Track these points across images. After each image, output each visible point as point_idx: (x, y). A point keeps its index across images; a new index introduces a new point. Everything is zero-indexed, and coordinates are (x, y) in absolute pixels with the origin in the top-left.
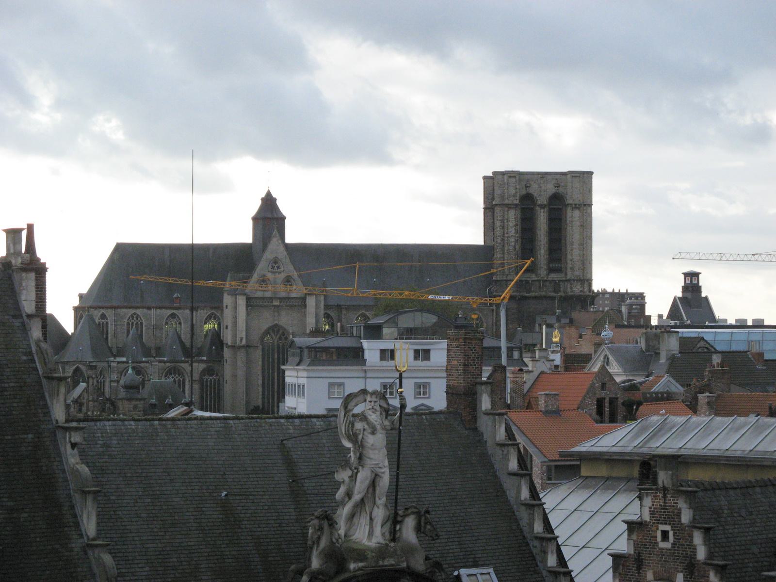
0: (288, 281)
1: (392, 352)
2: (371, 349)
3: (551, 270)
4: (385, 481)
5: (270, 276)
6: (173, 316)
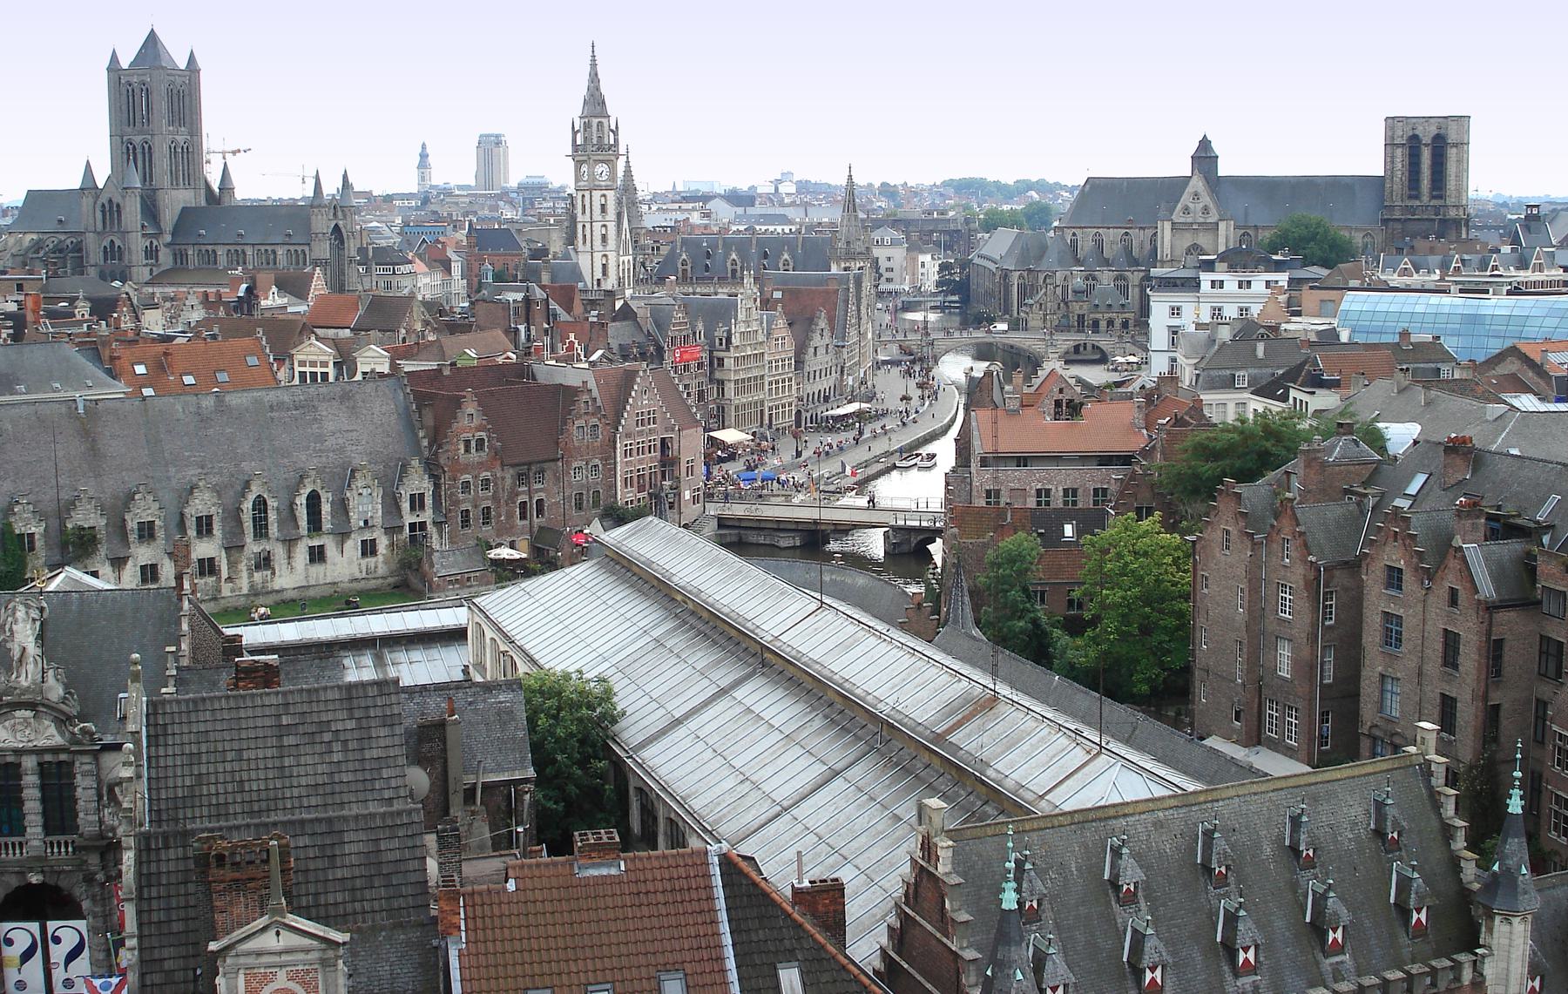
0: (1206, 210)
1: (1222, 282)
2: (1206, 278)
3: (1433, 197)
4: (32, 649)
5: (1191, 205)
6: (1127, 234)
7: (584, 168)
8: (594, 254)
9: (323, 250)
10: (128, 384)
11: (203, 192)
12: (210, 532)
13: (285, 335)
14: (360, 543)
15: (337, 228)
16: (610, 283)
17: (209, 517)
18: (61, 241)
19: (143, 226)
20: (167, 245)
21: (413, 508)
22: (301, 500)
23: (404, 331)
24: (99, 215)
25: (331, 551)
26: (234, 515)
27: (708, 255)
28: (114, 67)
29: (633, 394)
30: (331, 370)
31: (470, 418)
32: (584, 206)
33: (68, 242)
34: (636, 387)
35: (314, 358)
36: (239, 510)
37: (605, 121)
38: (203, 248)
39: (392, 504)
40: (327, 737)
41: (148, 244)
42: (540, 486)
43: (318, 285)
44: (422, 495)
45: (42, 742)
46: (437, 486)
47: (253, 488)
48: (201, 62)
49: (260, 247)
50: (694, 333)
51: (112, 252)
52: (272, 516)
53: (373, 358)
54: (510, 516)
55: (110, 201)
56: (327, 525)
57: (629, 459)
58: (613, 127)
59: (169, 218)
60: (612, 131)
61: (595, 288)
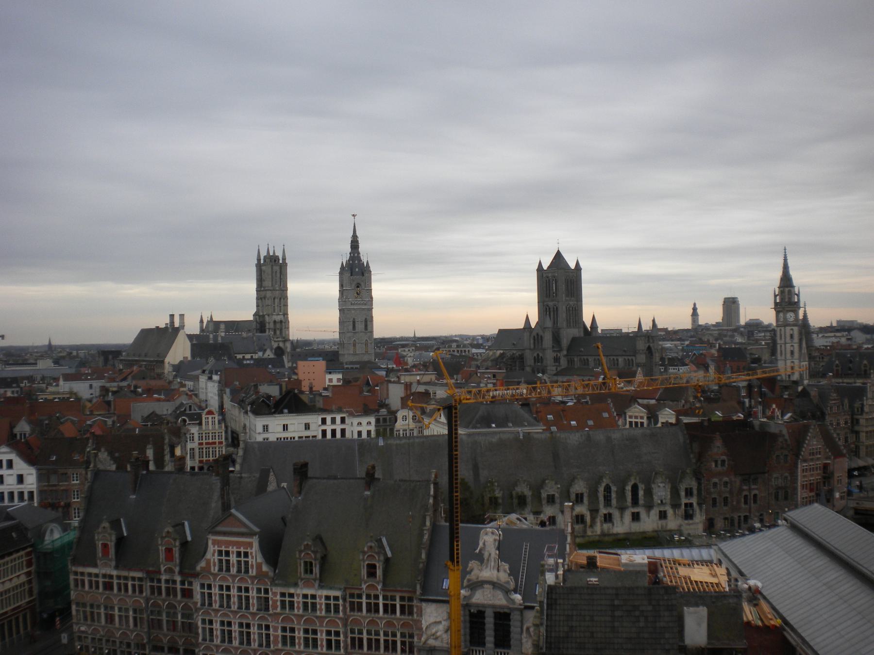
7: (781, 315)
8: (788, 361)
9: (642, 358)
10: (544, 425)
11: (582, 330)
12: (582, 501)
13: (624, 402)
14: (658, 512)
15: (649, 348)
16: (795, 377)
17: (582, 494)
18: (513, 354)
19: (553, 347)
20: (565, 356)
21: (686, 495)
22: (629, 488)
23: (683, 402)
24: (532, 341)
25: (643, 515)
26: (593, 494)
27: (851, 362)
28: (540, 269)
29: (808, 438)
30: (645, 421)
31: (718, 447)
32: (781, 335)
33: (517, 354)
34: (809, 434)
35: (637, 414)
36: (597, 491)
37: (791, 289)
38: (582, 357)
39: (675, 493)
40: (637, 613)
41: (555, 355)
42: (756, 487)
43: (640, 377)
44: (691, 489)
46: (699, 484)
47: (604, 480)
48: (582, 264)
49: (609, 357)
50: (843, 405)
51: (538, 359)
52: (614, 495)
53: (667, 416)
54: (738, 502)
55: (538, 335)
56: (641, 502)
57: (805, 474)
58: (797, 292)
59: (565, 343)
61: (787, 379)
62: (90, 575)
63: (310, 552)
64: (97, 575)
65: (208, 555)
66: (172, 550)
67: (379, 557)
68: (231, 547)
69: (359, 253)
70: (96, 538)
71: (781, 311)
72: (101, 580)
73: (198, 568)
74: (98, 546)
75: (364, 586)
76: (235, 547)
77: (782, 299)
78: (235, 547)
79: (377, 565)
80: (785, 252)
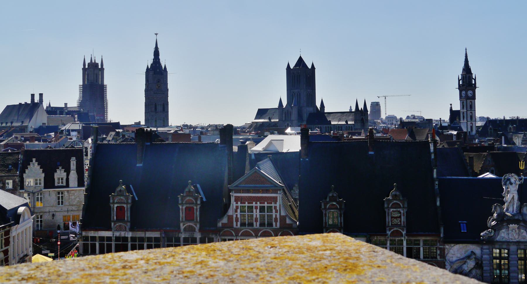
7: (464, 92)
8: (468, 122)
11: (315, 108)
24: (284, 116)
45: (523, 240)
55: (288, 111)
58: (474, 77)
60: (473, 79)
62: (102, 239)
63: (334, 203)
64: (109, 239)
65: (230, 212)
66: (194, 208)
67: (403, 205)
68: (254, 203)
69: (159, 60)
70: (111, 201)
71: (464, 90)
72: (113, 243)
73: (220, 225)
74: (114, 209)
75: (389, 233)
76: (258, 203)
77: (463, 82)
78: (258, 203)
79: (402, 212)
80: (466, 51)
